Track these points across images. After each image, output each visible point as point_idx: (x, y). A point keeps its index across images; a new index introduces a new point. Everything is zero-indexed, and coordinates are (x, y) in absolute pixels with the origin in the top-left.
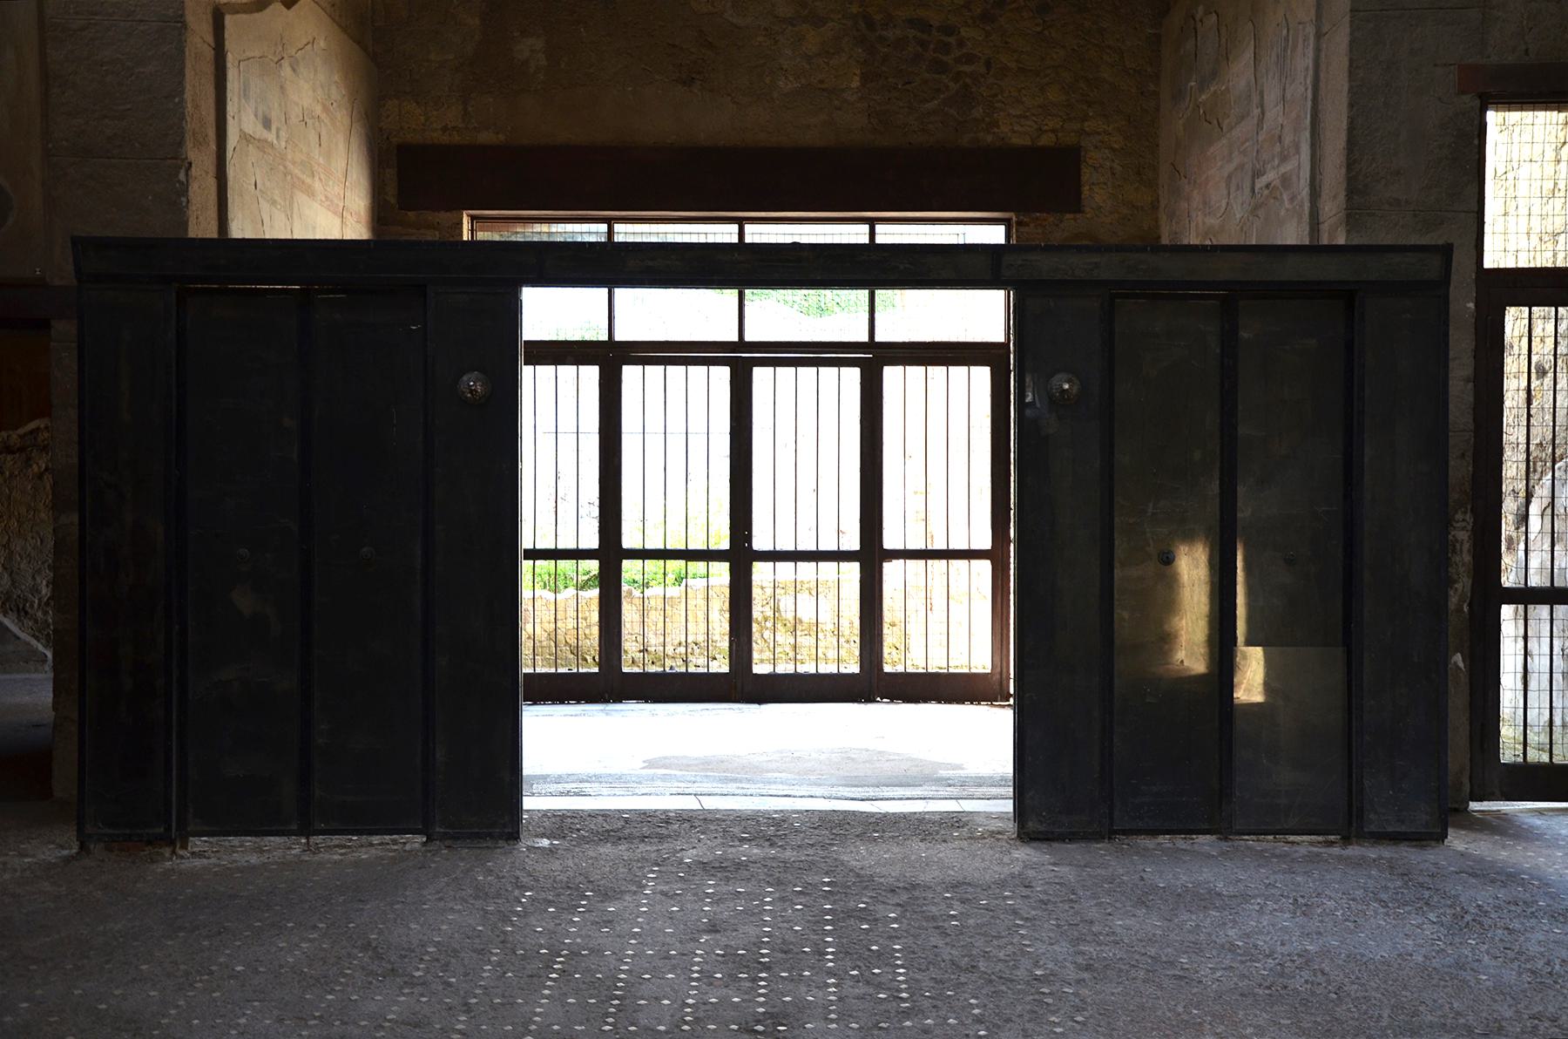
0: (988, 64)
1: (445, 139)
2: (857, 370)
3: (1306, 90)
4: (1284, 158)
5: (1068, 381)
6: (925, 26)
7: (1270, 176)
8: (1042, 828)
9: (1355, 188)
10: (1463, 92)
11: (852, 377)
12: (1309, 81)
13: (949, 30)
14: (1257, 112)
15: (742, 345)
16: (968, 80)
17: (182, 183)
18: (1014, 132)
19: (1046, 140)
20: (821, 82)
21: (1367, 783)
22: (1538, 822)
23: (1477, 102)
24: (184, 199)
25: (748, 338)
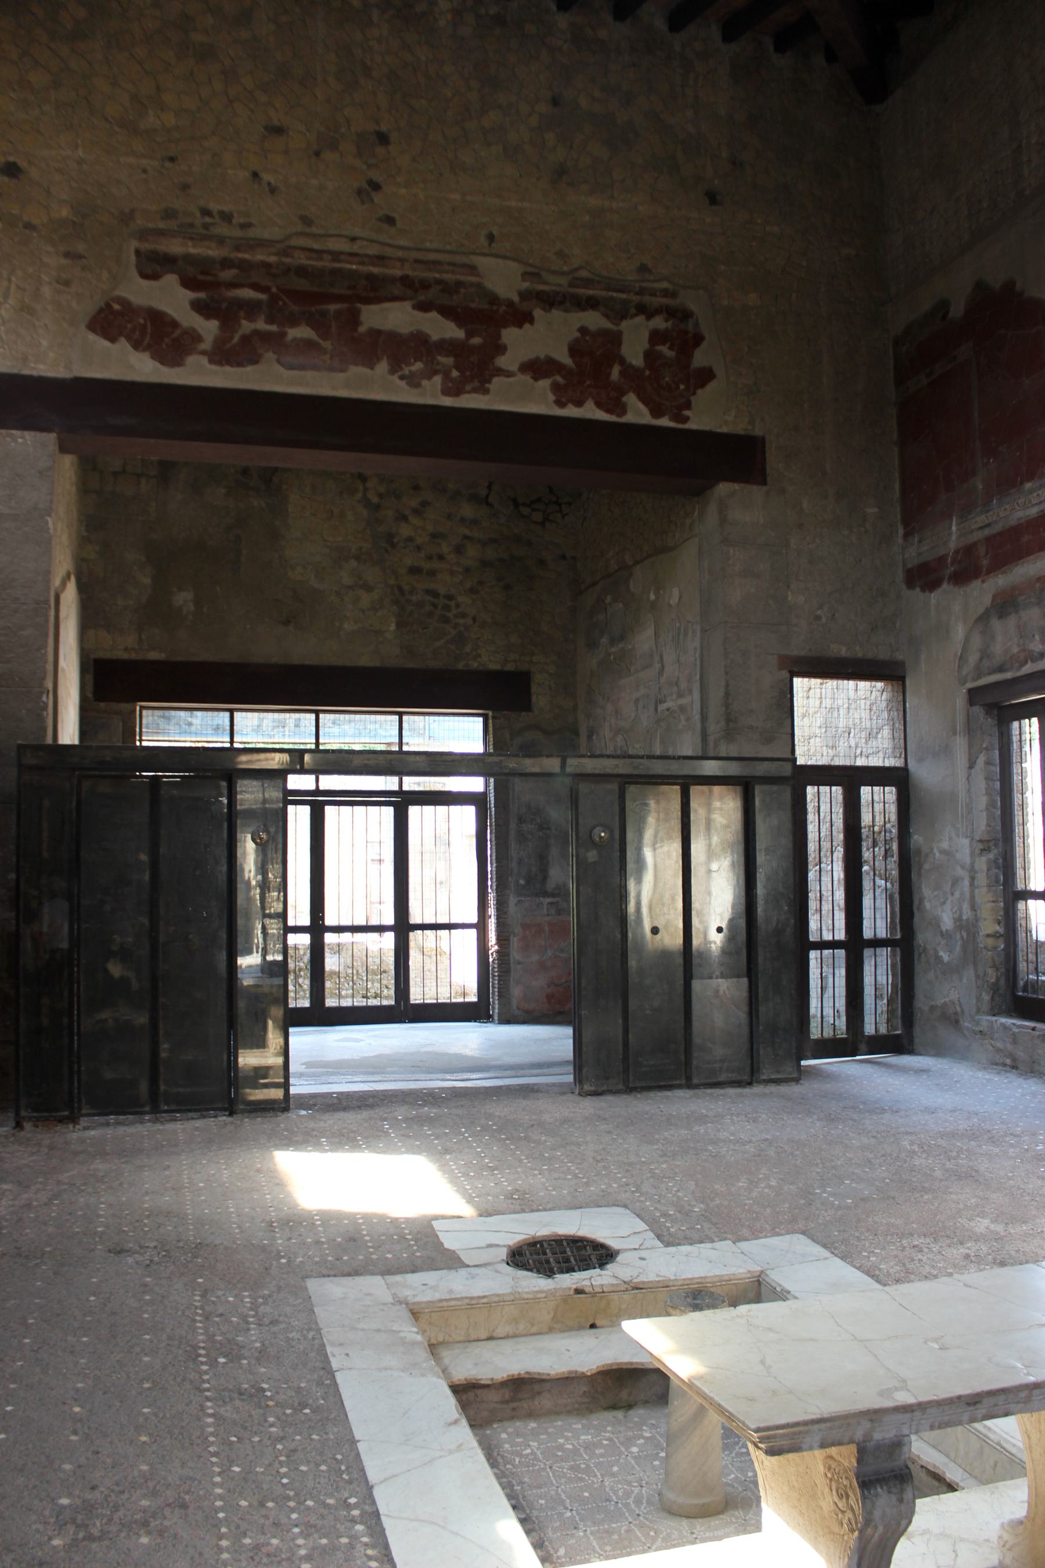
0: (474, 619)
1: (125, 656)
2: (391, 809)
3: (696, 660)
4: (680, 695)
5: (603, 831)
6: (435, 594)
7: (669, 704)
8: (592, 1088)
9: (730, 719)
10: (781, 668)
11: (389, 812)
12: (697, 655)
13: (450, 597)
14: (658, 666)
15: (317, 792)
16: (462, 629)
17: (44, 702)
18: (490, 661)
19: (510, 667)
20: (371, 626)
21: (761, 1052)
22: (834, 1069)
23: (788, 675)
24: (45, 713)
25: (321, 788)
